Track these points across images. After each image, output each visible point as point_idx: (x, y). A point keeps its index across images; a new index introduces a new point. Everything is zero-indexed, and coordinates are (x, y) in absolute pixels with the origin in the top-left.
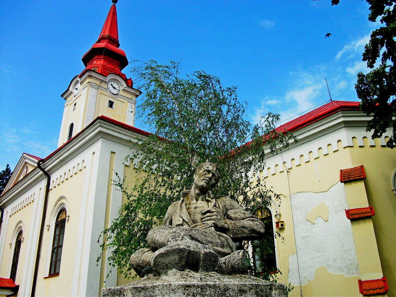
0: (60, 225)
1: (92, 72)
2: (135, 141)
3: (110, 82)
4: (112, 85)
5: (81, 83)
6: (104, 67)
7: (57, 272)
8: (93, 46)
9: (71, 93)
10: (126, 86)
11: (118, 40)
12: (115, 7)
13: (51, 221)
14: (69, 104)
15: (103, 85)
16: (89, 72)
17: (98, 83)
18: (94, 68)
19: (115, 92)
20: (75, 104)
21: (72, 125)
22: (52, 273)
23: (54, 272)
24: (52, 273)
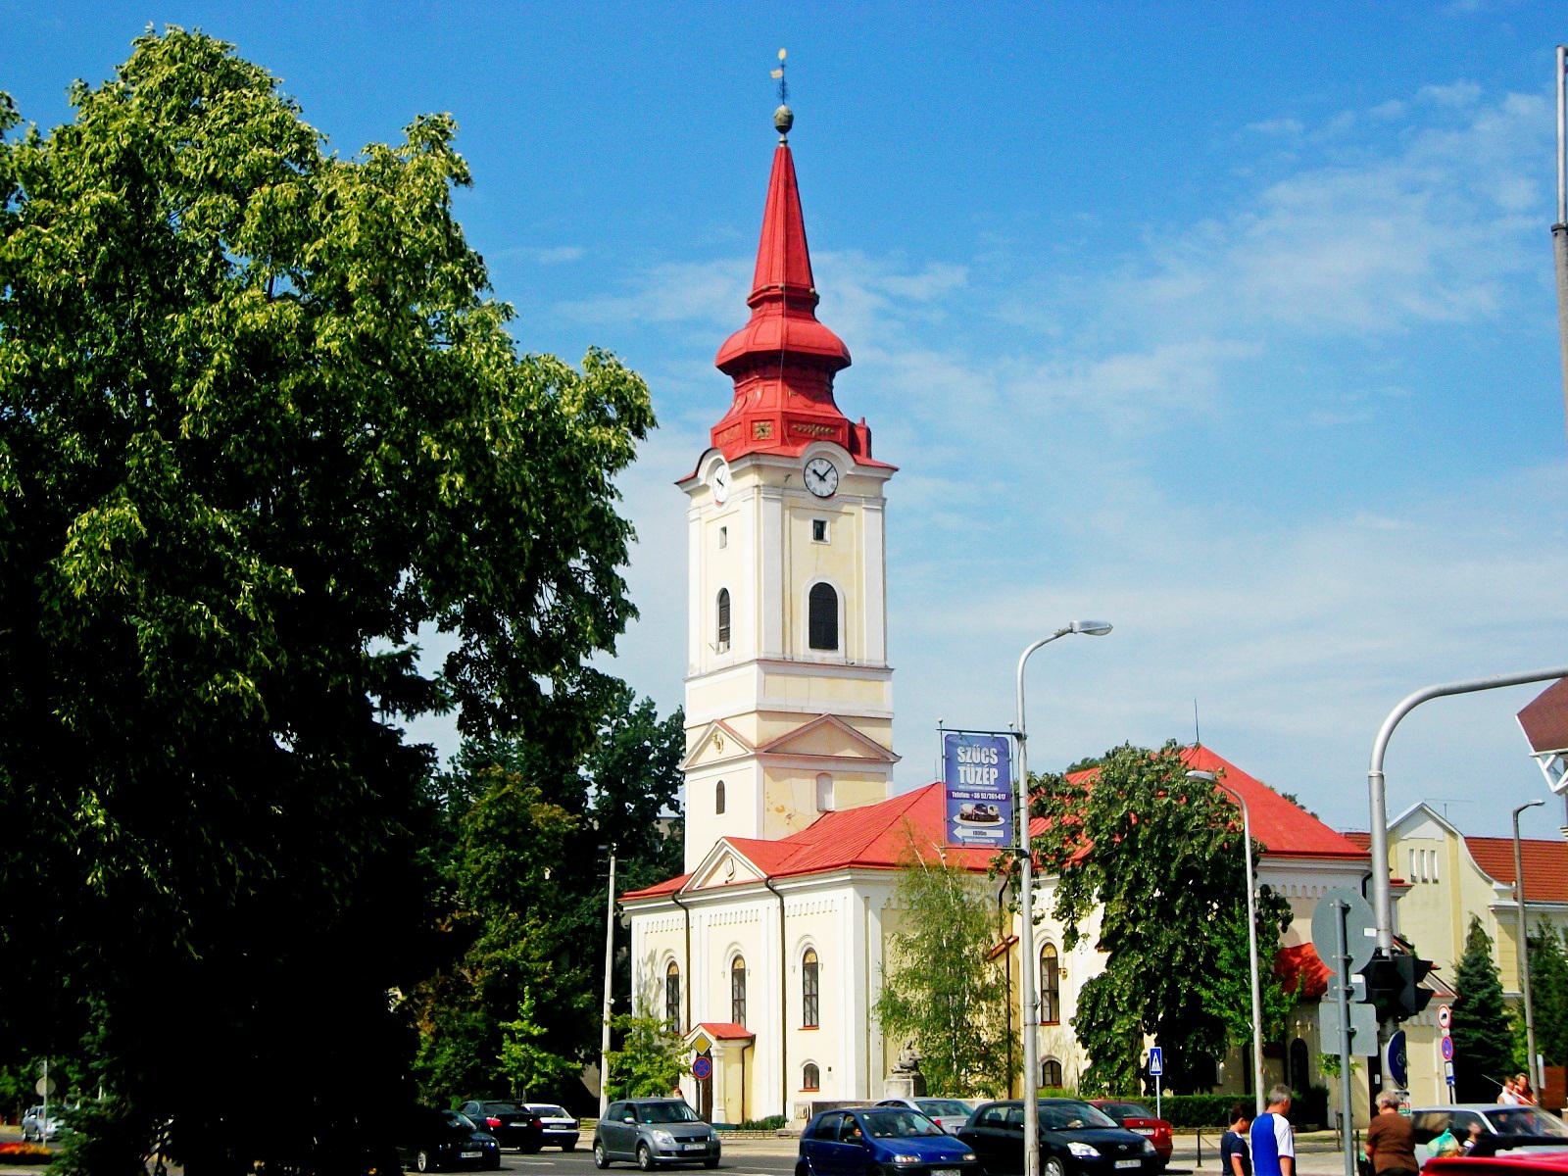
0: (811, 970)
1: (761, 457)
2: (888, 879)
3: (811, 465)
4: (815, 472)
5: (735, 476)
6: (789, 419)
7: (814, 1023)
8: (747, 343)
9: (705, 488)
10: (853, 464)
11: (812, 290)
12: (788, 151)
13: (795, 962)
14: (705, 518)
15: (797, 481)
16: (753, 456)
17: (779, 477)
18: (762, 424)
19: (825, 489)
20: (724, 530)
21: (724, 593)
22: (808, 1023)
23: (811, 1023)
24: (808, 1023)
